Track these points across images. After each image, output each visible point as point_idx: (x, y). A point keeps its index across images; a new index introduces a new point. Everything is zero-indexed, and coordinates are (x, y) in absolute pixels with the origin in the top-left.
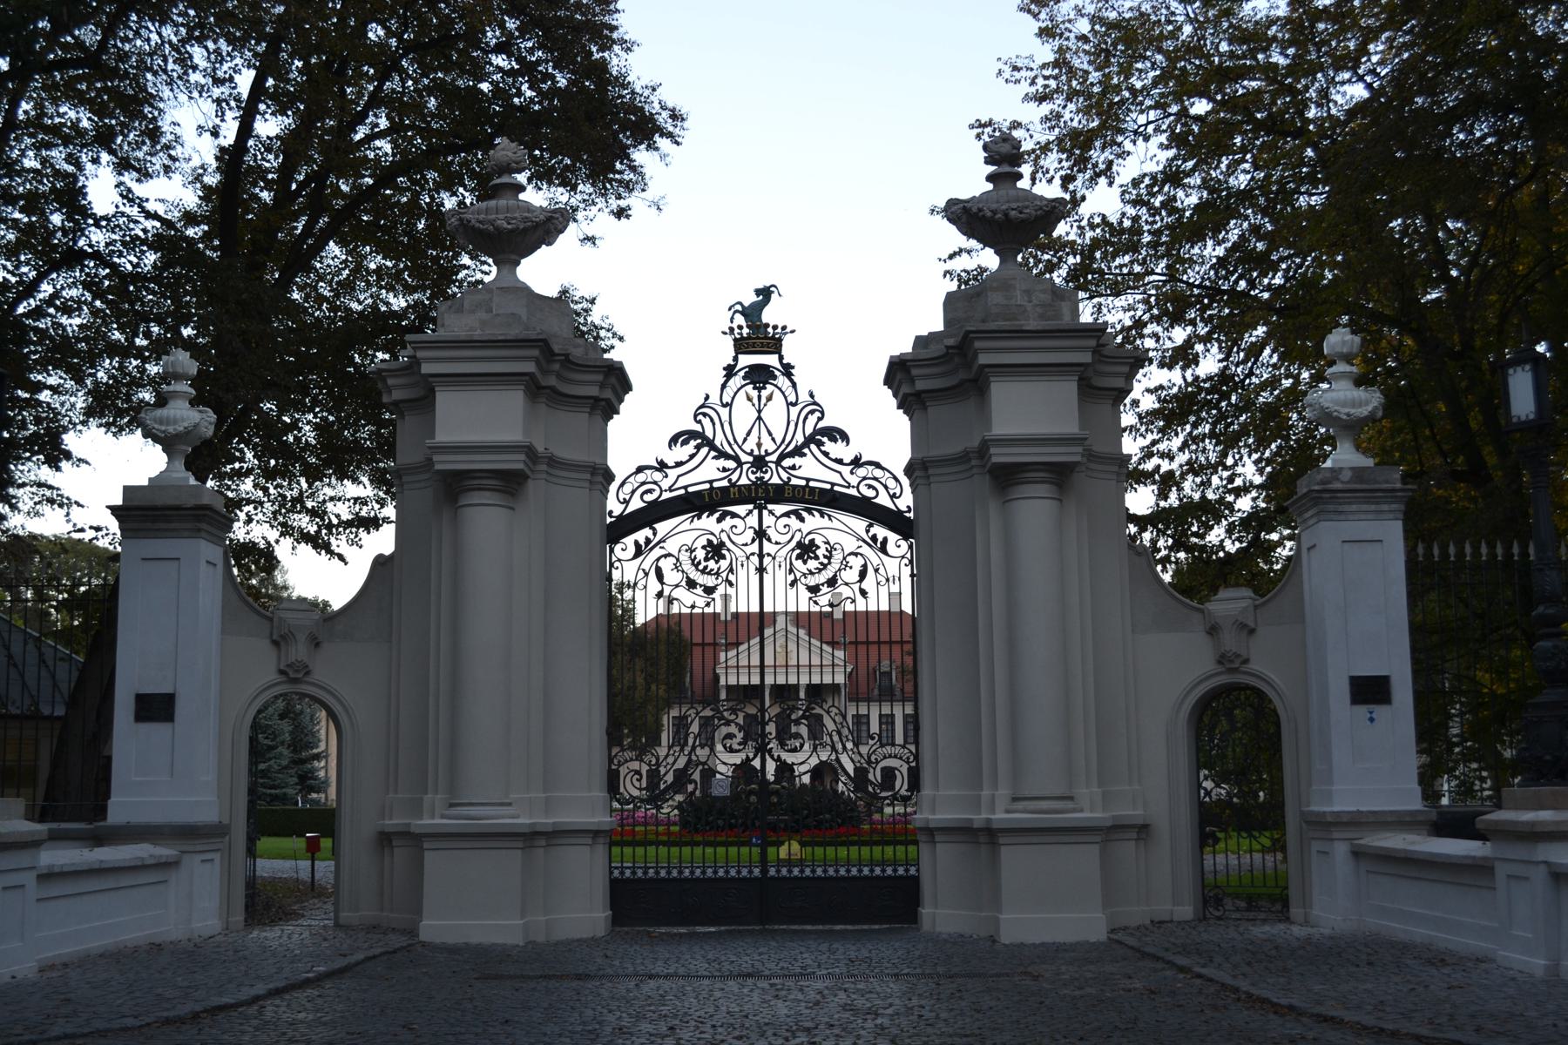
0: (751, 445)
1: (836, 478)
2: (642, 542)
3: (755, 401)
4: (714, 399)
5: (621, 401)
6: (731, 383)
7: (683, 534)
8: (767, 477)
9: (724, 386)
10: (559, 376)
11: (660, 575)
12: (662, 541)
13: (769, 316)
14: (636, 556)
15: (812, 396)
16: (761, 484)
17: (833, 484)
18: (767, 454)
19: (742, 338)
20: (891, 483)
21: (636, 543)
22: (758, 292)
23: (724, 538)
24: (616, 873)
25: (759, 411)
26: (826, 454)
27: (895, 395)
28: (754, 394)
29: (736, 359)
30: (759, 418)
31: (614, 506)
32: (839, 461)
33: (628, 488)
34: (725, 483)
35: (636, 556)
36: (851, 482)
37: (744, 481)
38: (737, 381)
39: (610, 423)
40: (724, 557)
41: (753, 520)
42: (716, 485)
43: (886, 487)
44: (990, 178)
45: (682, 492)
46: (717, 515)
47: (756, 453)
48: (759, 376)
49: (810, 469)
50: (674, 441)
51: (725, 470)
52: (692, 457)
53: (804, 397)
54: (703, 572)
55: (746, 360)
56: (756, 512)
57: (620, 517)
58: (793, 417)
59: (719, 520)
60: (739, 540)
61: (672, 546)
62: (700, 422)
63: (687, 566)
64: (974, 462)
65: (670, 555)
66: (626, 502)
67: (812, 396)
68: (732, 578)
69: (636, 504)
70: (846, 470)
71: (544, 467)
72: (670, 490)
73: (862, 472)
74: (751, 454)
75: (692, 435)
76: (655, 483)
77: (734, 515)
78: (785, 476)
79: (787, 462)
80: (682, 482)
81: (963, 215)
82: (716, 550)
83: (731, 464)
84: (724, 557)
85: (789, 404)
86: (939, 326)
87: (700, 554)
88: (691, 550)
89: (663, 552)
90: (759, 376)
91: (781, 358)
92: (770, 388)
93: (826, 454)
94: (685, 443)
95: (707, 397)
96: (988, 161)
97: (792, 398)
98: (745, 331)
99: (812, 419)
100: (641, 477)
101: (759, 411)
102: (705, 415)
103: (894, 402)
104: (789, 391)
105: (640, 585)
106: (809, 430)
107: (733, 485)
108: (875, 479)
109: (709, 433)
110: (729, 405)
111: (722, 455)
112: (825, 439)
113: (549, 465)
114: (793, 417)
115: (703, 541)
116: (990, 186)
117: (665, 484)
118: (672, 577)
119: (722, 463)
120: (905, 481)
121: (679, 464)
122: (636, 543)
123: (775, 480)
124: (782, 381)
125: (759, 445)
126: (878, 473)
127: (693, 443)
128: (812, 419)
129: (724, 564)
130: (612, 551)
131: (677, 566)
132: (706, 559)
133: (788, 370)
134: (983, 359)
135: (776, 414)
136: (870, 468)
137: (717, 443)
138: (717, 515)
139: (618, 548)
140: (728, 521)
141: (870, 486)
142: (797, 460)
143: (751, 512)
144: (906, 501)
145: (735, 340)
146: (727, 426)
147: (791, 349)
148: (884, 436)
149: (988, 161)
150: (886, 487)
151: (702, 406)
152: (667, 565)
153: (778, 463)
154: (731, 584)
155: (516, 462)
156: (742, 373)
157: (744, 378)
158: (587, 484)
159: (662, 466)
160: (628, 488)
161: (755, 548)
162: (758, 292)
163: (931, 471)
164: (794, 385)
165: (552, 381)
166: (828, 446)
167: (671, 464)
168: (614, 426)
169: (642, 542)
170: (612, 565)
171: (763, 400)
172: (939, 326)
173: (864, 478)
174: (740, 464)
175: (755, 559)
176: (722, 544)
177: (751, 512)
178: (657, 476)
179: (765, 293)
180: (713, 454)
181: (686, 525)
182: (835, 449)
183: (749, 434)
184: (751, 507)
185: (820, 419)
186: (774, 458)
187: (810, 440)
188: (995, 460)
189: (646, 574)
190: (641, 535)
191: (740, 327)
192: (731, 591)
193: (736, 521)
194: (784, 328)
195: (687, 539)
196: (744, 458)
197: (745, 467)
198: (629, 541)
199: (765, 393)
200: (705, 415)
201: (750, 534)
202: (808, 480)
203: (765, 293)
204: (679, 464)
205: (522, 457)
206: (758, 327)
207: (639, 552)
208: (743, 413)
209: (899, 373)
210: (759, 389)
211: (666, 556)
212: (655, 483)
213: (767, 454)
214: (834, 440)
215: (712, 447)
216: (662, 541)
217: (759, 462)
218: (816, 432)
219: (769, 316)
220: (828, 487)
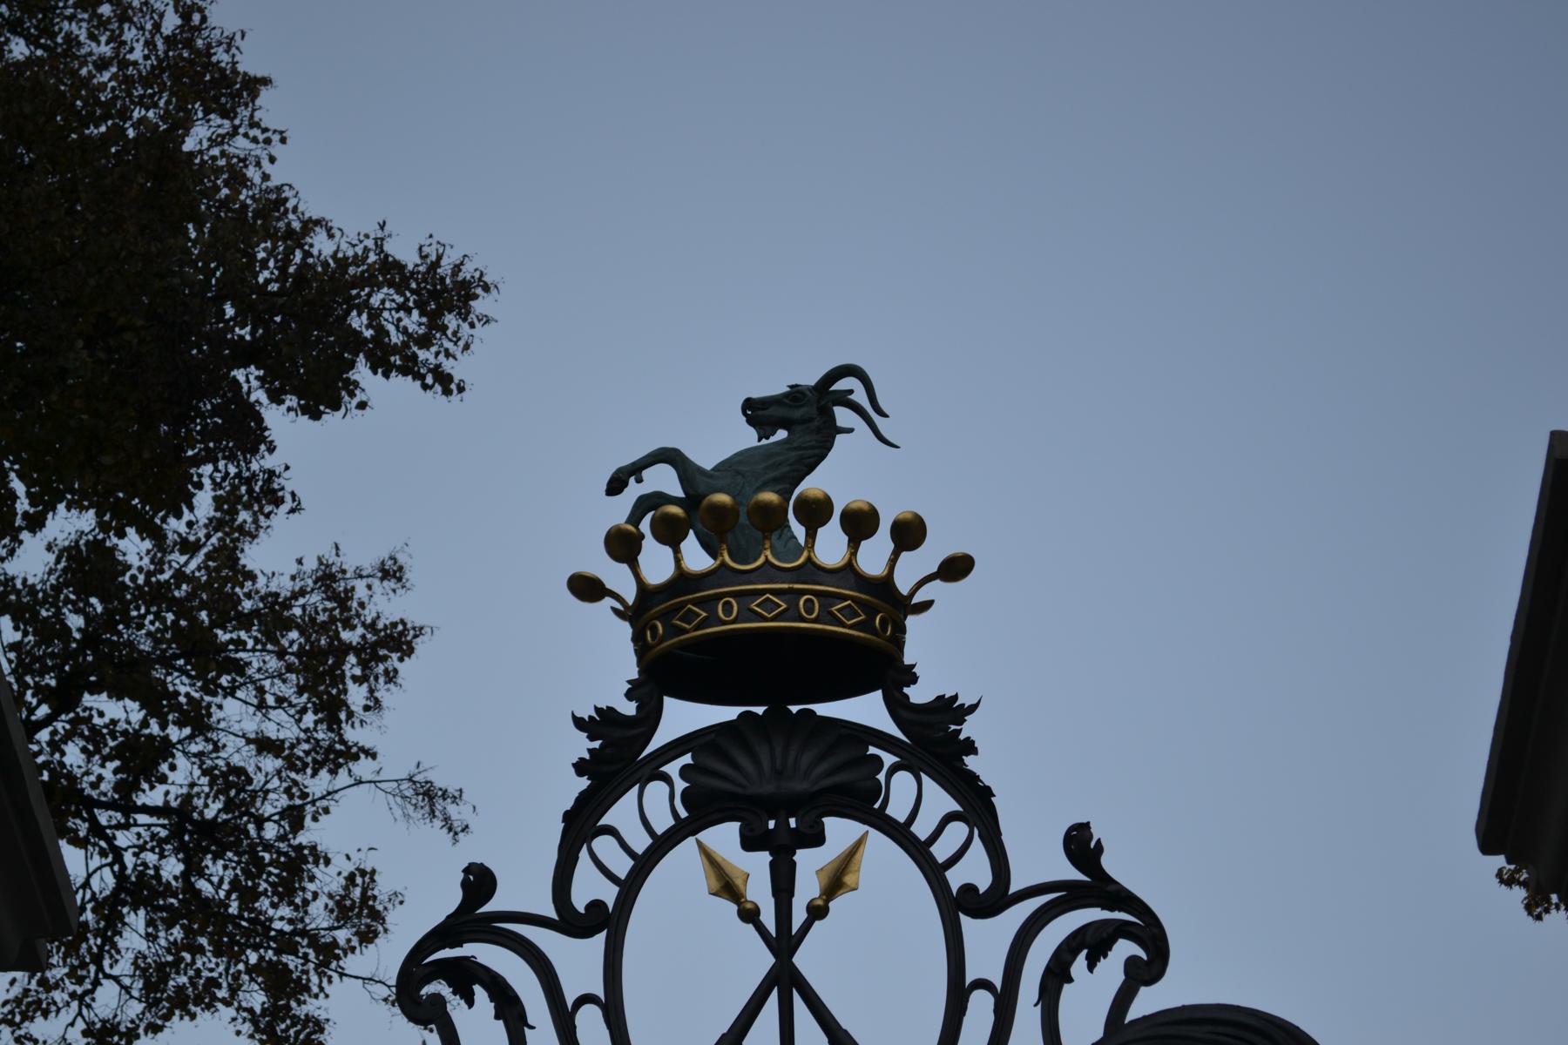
3: (760, 892)
4: (523, 889)
6: (622, 814)
9: (582, 824)
15: (1080, 844)
19: (683, 581)
22: (758, 412)
25: (784, 943)
28: (756, 868)
53: (1038, 859)
67: (1080, 844)
85: (958, 906)
91: (897, 705)
92: (840, 831)
95: (479, 882)
97: (974, 871)
101: (784, 943)
102: (466, 977)
110: (606, 922)
124: (910, 794)
133: (937, 739)
162: (758, 412)
164: (977, 806)
171: (807, 888)
179: (803, 419)
194: (909, 534)
199: (810, 864)
200: (466, 977)
203: (803, 419)
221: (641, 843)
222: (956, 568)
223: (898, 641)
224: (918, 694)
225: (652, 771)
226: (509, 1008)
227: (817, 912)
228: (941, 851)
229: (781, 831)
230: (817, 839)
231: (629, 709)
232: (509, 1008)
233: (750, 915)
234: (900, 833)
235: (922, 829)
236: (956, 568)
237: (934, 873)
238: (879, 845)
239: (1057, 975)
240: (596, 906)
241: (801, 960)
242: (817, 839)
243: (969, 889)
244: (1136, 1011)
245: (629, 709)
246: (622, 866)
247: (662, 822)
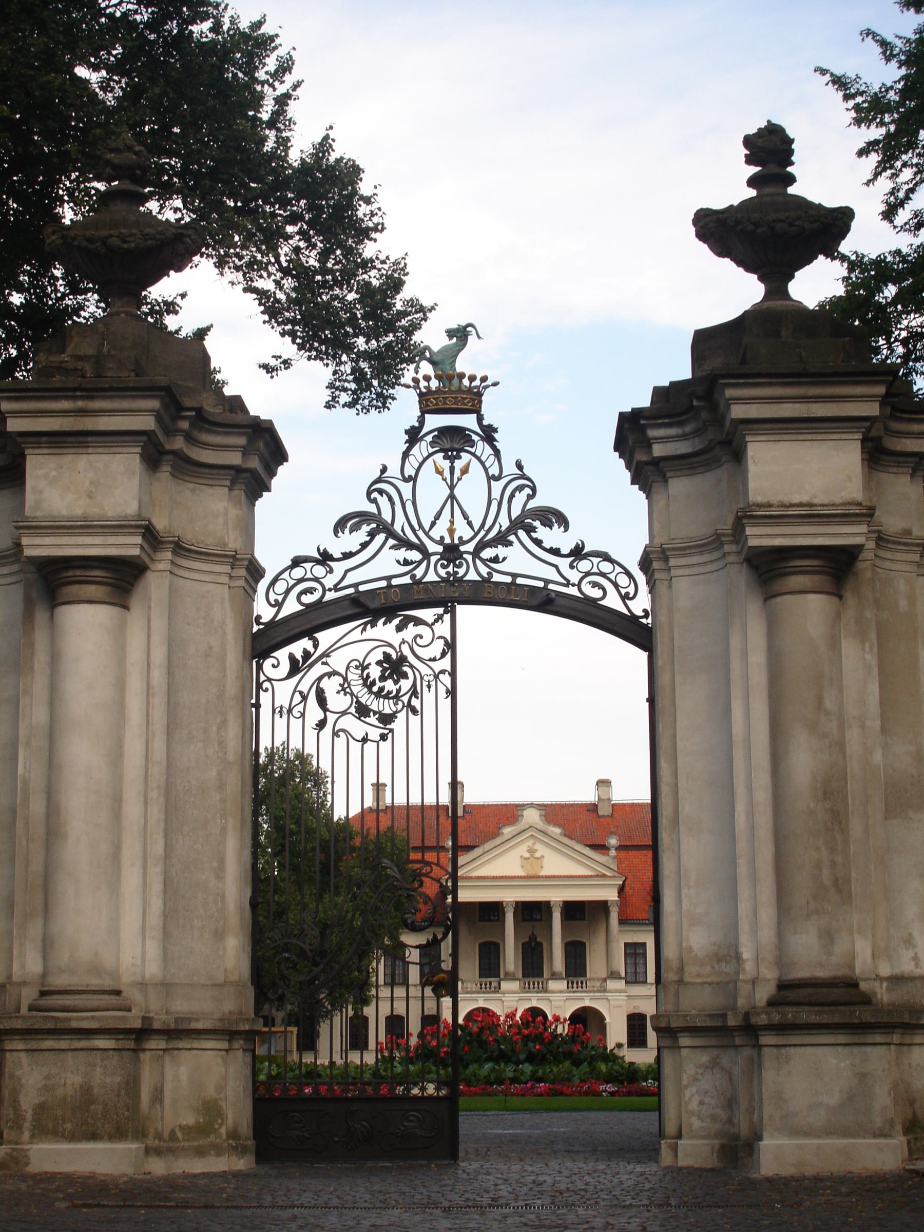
0: (440, 530)
1: (550, 574)
2: (299, 656)
3: (447, 474)
4: (394, 471)
5: (273, 474)
6: (415, 450)
7: (352, 646)
8: (461, 572)
9: (406, 455)
10: (190, 439)
11: (322, 701)
12: (326, 654)
13: (464, 364)
14: (291, 674)
15: (519, 466)
16: (454, 581)
17: (547, 582)
18: (462, 542)
20: (623, 580)
21: (292, 658)
22: (450, 333)
23: (406, 650)
24: (261, 1091)
25: (452, 487)
26: (538, 543)
27: (628, 467)
28: (446, 464)
29: (422, 421)
30: (452, 497)
31: (264, 611)
32: (556, 552)
33: (281, 587)
34: (407, 580)
35: (291, 674)
36: (569, 578)
37: (431, 577)
38: (421, 449)
39: (259, 503)
40: (405, 676)
41: (443, 629)
42: (395, 582)
43: (616, 585)
44: (752, 182)
45: (351, 591)
46: (396, 621)
47: (448, 540)
48: (453, 442)
49: (519, 562)
50: (340, 526)
51: (406, 563)
52: (364, 546)
53: (510, 469)
54: (379, 694)
55: (434, 421)
56: (447, 617)
57: (272, 624)
58: (496, 494)
59: (399, 629)
60: (424, 653)
61: (338, 661)
62: (374, 501)
63: (357, 688)
64: (727, 548)
65: (335, 673)
66: (279, 605)
67: (519, 466)
68: (415, 702)
69: (291, 607)
70: (563, 563)
71: (168, 555)
72: (336, 588)
73: (584, 565)
74: (441, 541)
75: (362, 517)
76: (316, 580)
77: (418, 622)
78: (484, 571)
79: (487, 553)
80: (351, 579)
81: (718, 230)
82: (394, 666)
83: (415, 555)
84: (405, 676)
85: (491, 478)
86: (685, 373)
87: (375, 672)
88: (363, 667)
89: (327, 669)
90: (453, 442)
91: (480, 419)
93: (538, 543)
94: (355, 528)
95: (384, 469)
96: (749, 160)
97: (494, 471)
98: (434, 384)
99: (520, 498)
100: (298, 573)
101: (452, 487)
102: (381, 492)
103: (627, 475)
104: (491, 461)
105: (295, 712)
106: (515, 513)
107: (417, 582)
108: (603, 575)
109: (387, 516)
110: (413, 479)
111: (403, 543)
112: (537, 523)
113: (175, 552)
114: (496, 494)
115: (378, 655)
116: (752, 193)
117: (329, 582)
118: (337, 702)
119: (403, 554)
120: (641, 578)
121: (347, 556)
122: (292, 658)
123: (472, 576)
124: (482, 448)
125: (451, 531)
126: (606, 567)
127: (365, 528)
128: (520, 498)
129: (405, 685)
130: (260, 668)
131: (345, 688)
132: (383, 678)
133: (489, 434)
134: (738, 412)
135: (473, 491)
136: (596, 560)
137: (397, 528)
138: (396, 621)
139: (267, 664)
140: (411, 631)
141: (595, 585)
142: (501, 551)
143: (440, 618)
144: (641, 604)
145: (421, 395)
146: (409, 506)
147: (493, 408)
148: (613, 516)
149: (749, 160)
150: (616, 585)
151: (375, 482)
152: (331, 686)
153: (476, 553)
154: (414, 711)
155: (128, 546)
156: (429, 438)
157: (432, 444)
158: (225, 579)
159: (325, 558)
160: (281, 587)
161: (446, 663)
162: (450, 333)
163: (672, 562)
164: (497, 453)
165: (179, 443)
166: (542, 532)
167: (337, 555)
168: (263, 505)
169: (299, 656)
170: (259, 686)
171: (457, 473)
172: (685, 373)
173: (588, 574)
174: (426, 555)
175: (446, 679)
176: (403, 659)
177: (440, 618)
178: (319, 571)
180: (391, 542)
182: (551, 536)
183: (438, 516)
184: (440, 610)
185: (530, 497)
186: (470, 547)
187: (518, 524)
188: (752, 542)
189: (304, 698)
190: (298, 648)
191: (427, 378)
192: (414, 720)
193: (421, 629)
194: (484, 379)
195: (358, 652)
196: (432, 547)
197: (434, 559)
198: (282, 655)
199: (459, 464)
200: (381, 492)
201: (439, 645)
202: (515, 576)
204: (347, 556)
205: (139, 540)
206: (450, 378)
207: (295, 668)
208: (431, 491)
209: (632, 433)
210: (452, 459)
211: (329, 675)
212: (316, 580)
213: (462, 542)
214: (548, 524)
215: (391, 534)
216: (326, 654)
217: (452, 553)
218: (525, 513)
219: (464, 364)
220: (541, 584)
221: (421, 459)
222: (495, 384)
223: (480, 407)
224: (485, 423)
225: (422, 439)
226: (390, 499)
227: (459, 479)
228: (487, 464)
229: (452, 454)
230: (460, 458)
231: (417, 425)
232: (390, 499)
233: (445, 480)
234: (479, 459)
235: (483, 458)
236: (495, 384)
237: (486, 470)
238: (474, 460)
239: (512, 496)
240: (410, 476)
241: (456, 492)
242: (460, 458)
243: (493, 475)
244: (528, 507)
245: (417, 425)
246: (416, 465)
247: (425, 454)
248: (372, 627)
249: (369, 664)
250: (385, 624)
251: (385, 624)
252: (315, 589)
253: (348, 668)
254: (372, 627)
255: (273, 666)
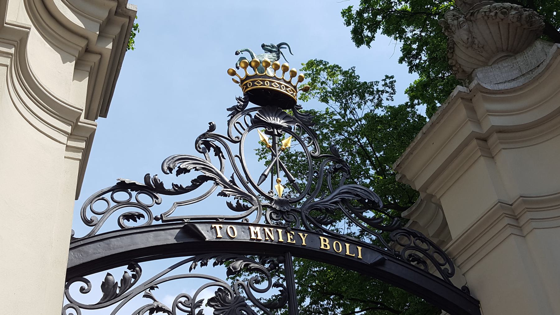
4: (221, 130)
95: (212, 127)
100: (122, 196)
115: (209, 293)
121: (179, 190)
139: (76, 286)
146: (237, 160)
167: (168, 186)
178: (145, 199)
181: (184, 269)
195: (189, 287)
198: (96, 279)
248: (202, 265)
249: (201, 301)
250: (215, 264)
251: (215, 264)
252: (140, 216)
253: (175, 305)
254: (202, 265)
255: (82, 290)
